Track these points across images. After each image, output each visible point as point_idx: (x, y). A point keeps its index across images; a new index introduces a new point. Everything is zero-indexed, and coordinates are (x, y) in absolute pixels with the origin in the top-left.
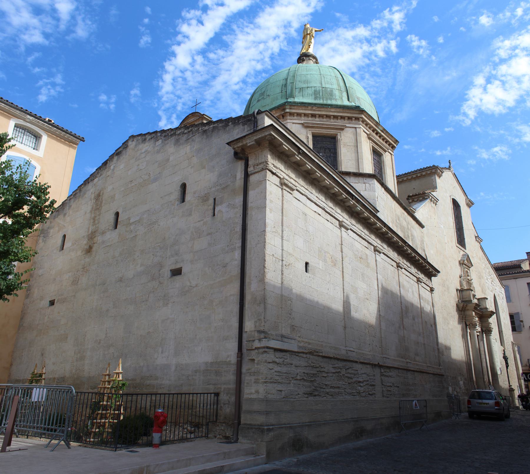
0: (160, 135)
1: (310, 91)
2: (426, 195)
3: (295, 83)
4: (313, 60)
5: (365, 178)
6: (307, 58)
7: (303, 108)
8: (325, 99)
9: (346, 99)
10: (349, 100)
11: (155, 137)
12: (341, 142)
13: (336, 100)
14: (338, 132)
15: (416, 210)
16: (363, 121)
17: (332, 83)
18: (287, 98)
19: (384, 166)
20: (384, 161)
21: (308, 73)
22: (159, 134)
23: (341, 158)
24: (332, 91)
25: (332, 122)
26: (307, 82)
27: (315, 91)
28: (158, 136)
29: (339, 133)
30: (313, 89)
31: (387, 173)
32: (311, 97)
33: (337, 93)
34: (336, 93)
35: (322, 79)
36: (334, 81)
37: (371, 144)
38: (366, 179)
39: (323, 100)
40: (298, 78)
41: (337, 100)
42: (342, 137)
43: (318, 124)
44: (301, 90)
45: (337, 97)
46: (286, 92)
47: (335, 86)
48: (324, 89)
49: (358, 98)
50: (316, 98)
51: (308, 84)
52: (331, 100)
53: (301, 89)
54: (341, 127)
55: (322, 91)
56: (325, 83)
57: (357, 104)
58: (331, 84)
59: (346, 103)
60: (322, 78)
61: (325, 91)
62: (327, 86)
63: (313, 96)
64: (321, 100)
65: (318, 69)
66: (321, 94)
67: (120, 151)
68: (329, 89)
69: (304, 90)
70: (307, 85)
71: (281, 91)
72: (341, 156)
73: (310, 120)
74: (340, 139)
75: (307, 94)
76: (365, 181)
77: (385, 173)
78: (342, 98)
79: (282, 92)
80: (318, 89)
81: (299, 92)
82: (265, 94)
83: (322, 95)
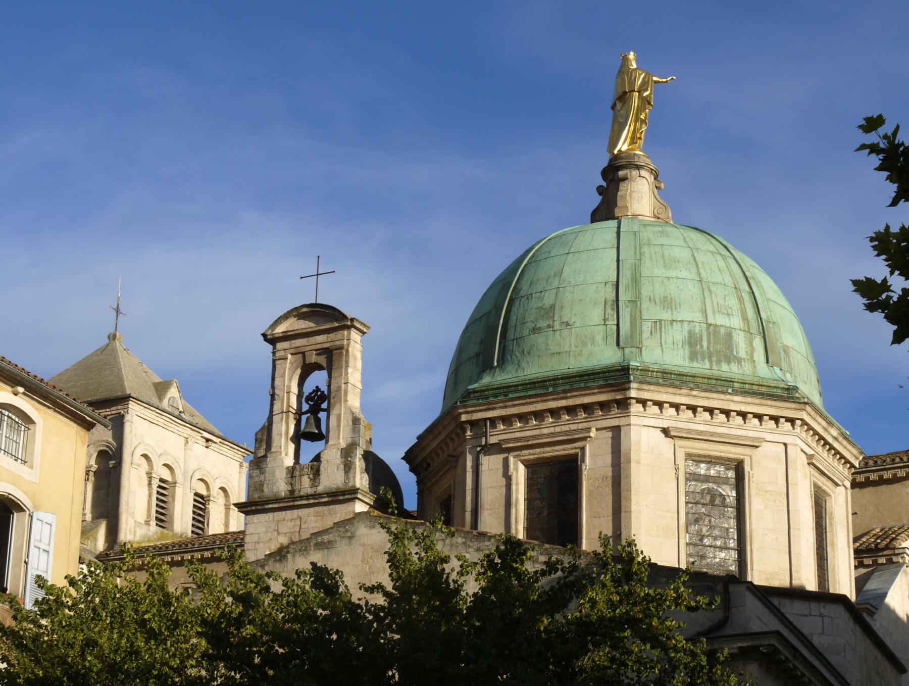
0: (464, 543)
1: (678, 334)
2: (897, 551)
3: (639, 303)
4: (649, 179)
5: (822, 604)
6: (635, 173)
7: (671, 390)
8: (714, 359)
9: (763, 359)
10: (767, 362)
11: (447, 542)
12: (751, 481)
13: (739, 361)
14: (746, 455)
15: (877, 609)
16: (804, 423)
17: (730, 313)
18: (621, 344)
19: (831, 525)
20: (832, 514)
21: (671, 273)
22: (460, 540)
23: (750, 523)
24: (729, 335)
25: (736, 428)
26: (668, 303)
27: (691, 334)
28: (457, 543)
29: (745, 457)
30: (686, 327)
31: (837, 545)
32: (681, 352)
33: (740, 339)
34: (740, 340)
35: (706, 296)
36: (733, 302)
37: (812, 478)
38: (824, 607)
39: (711, 361)
40: (646, 290)
41: (743, 363)
42: (754, 468)
43: (702, 432)
44: (656, 326)
45: (742, 354)
46: (618, 325)
47: (736, 322)
48: (712, 328)
49: (785, 351)
50: (693, 356)
51: (674, 311)
52: (729, 363)
53: (658, 324)
54: (753, 441)
55: (709, 334)
56: (714, 311)
57: (790, 380)
58: (728, 314)
59: (763, 371)
60: (707, 293)
61: (714, 335)
62: (720, 320)
63: (687, 352)
64: (707, 361)
65: (692, 261)
66: (705, 344)
67: (330, 542)
68: (722, 330)
69: (663, 330)
70: (670, 313)
71: (605, 320)
72: (750, 518)
73: (683, 421)
74: (749, 472)
75: (670, 341)
76: (822, 610)
77: (833, 545)
78: (752, 356)
79: (605, 324)
80: (697, 330)
81: (651, 333)
82: (556, 318)
83: (708, 348)
